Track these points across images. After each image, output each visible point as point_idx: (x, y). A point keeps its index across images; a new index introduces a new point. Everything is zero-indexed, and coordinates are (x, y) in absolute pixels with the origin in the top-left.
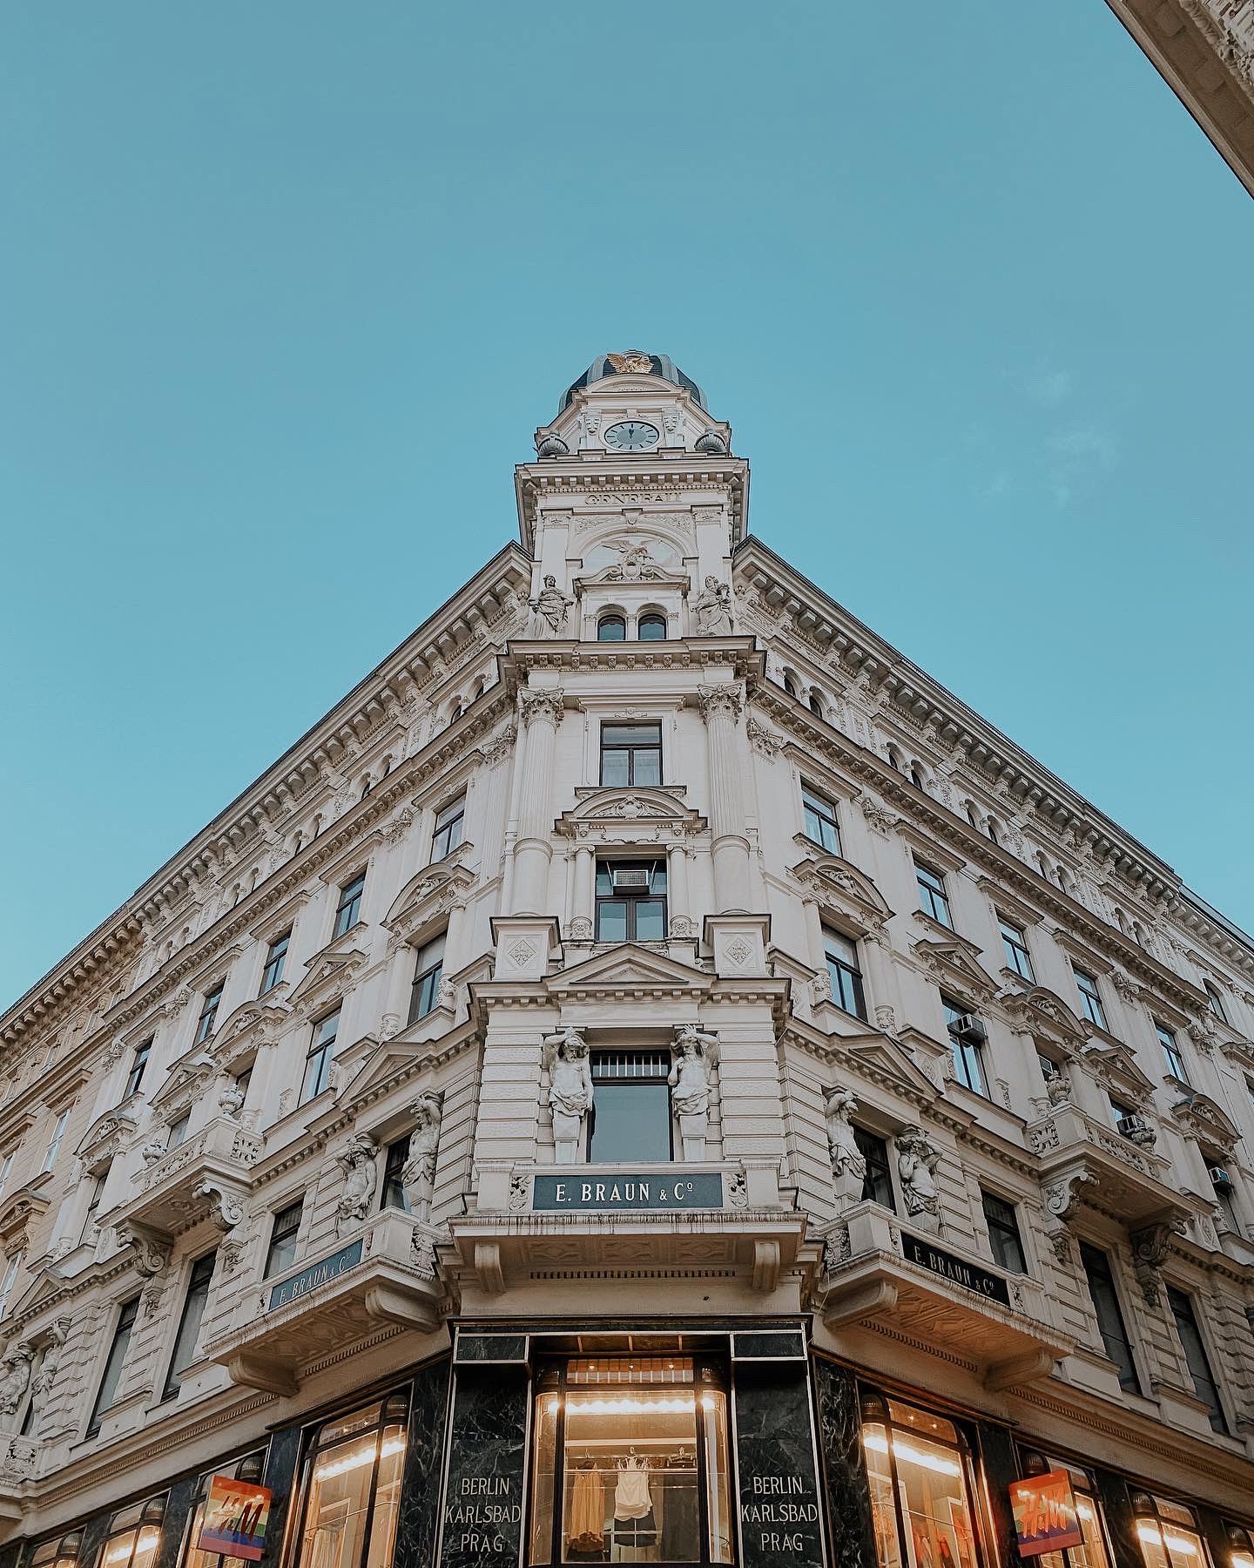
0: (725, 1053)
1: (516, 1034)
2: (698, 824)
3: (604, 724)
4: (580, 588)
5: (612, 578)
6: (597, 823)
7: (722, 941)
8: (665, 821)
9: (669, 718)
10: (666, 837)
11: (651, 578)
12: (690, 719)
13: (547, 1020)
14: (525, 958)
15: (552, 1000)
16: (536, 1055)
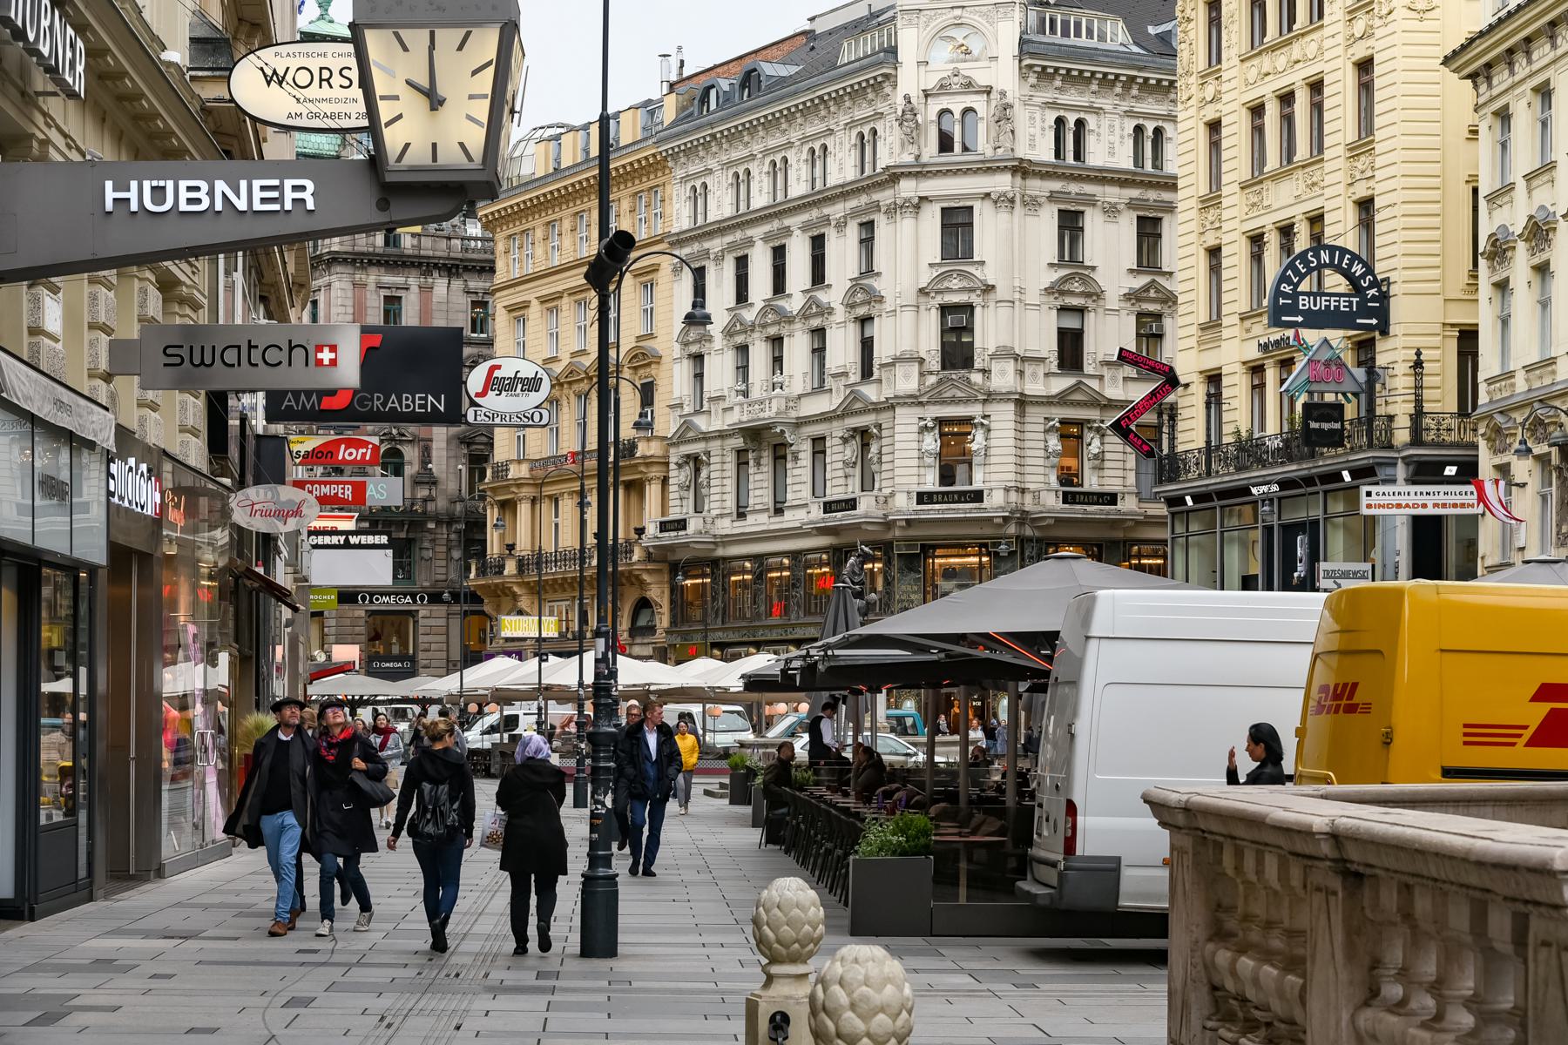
0: (993, 426)
1: (906, 423)
2: (989, 289)
3: (943, 209)
4: (927, 94)
5: (943, 89)
6: (939, 292)
7: (995, 367)
8: (972, 290)
9: (977, 205)
10: (974, 298)
11: (969, 86)
12: (988, 205)
13: (919, 411)
14: (906, 381)
15: (921, 404)
16: (915, 428)
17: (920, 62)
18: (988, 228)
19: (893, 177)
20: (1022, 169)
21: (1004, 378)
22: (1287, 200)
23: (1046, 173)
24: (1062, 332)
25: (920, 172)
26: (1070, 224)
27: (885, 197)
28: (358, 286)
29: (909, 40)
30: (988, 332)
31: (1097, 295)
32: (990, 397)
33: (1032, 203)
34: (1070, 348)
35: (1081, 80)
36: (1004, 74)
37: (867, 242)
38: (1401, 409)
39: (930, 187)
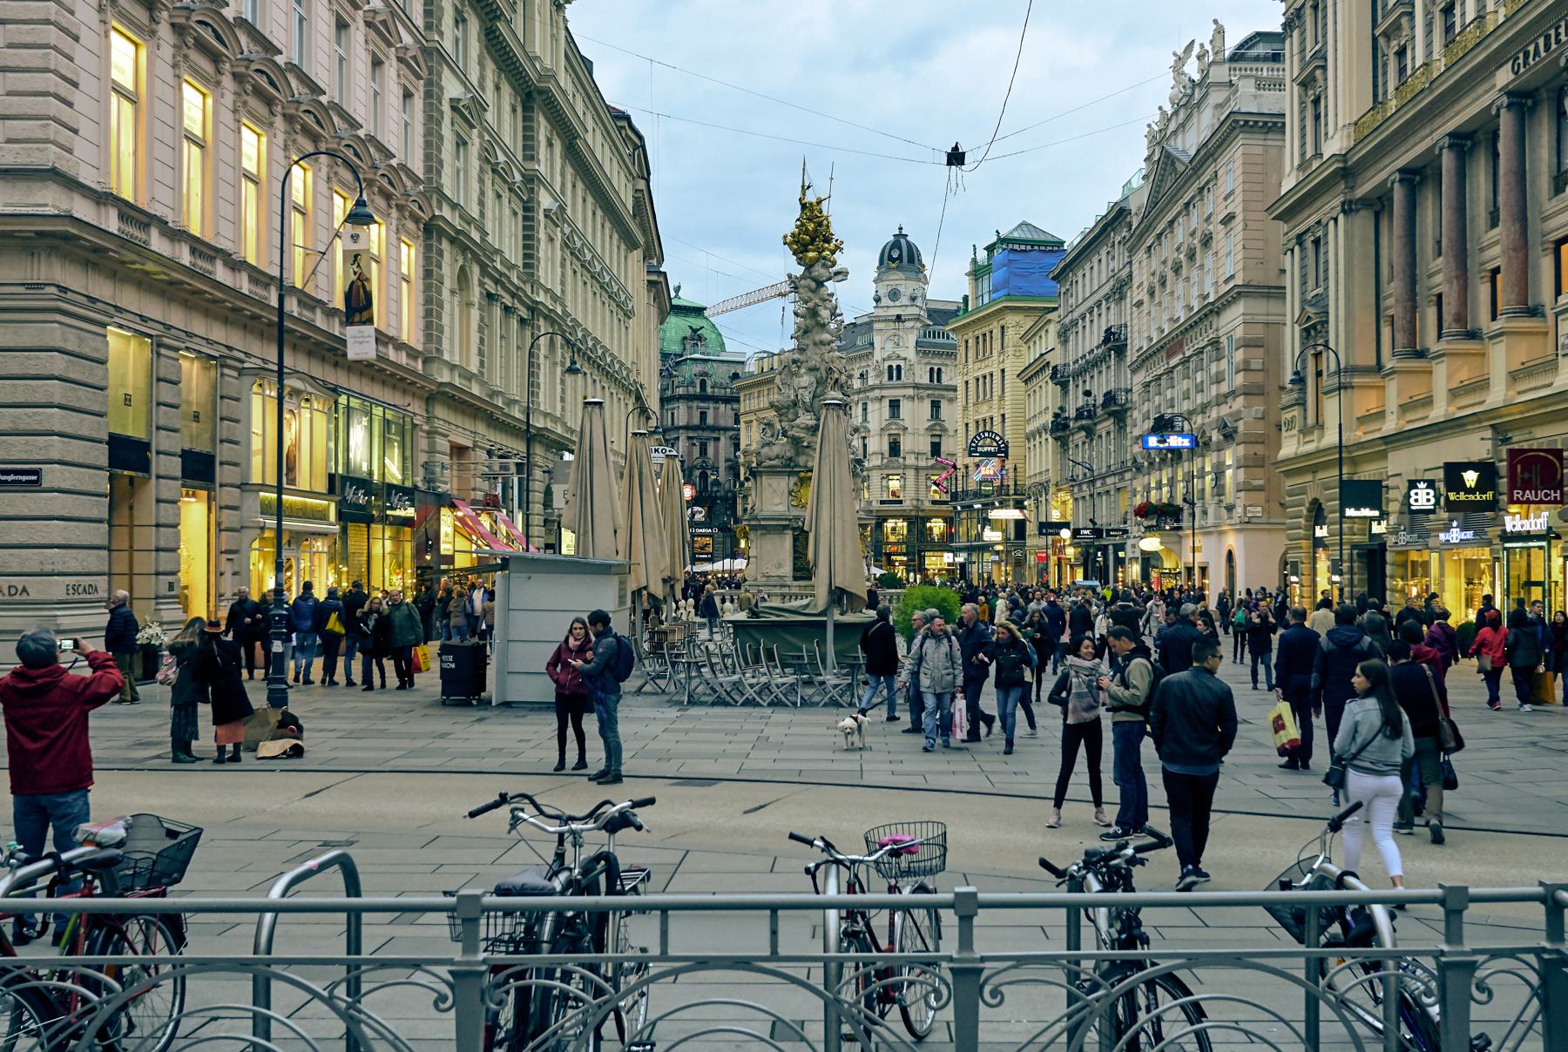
5: (889, 358)
17: (883, 347)
18: (905, 407)
19: (873, 388)
20: (916, 387)
21: (911, 460)
22: (984, 412)
23: (926, 388)
24: (933, 444)
25: (881, 387)
26: (936, 406)
27: (871, 394)
28: (690, 408)
29: (877, 340)
30: (906, 444)
31: (945, 430)
32: (905, 467)
33: (921, 399)
34: (936, 449)
35: (940, 355)
36: (911, 353)
37: (865, 409)
38: (1012, 483)
39: (884, 393)
